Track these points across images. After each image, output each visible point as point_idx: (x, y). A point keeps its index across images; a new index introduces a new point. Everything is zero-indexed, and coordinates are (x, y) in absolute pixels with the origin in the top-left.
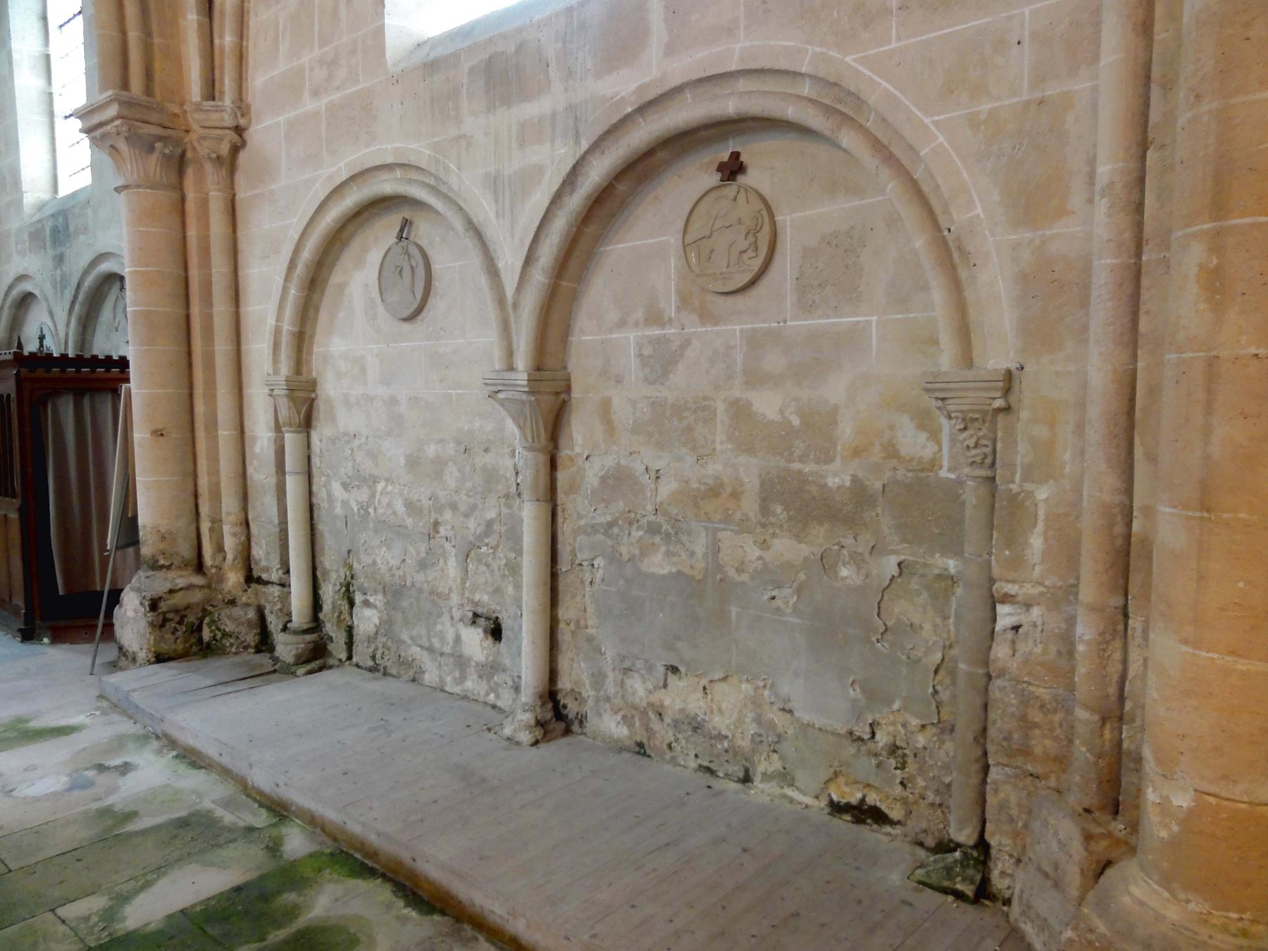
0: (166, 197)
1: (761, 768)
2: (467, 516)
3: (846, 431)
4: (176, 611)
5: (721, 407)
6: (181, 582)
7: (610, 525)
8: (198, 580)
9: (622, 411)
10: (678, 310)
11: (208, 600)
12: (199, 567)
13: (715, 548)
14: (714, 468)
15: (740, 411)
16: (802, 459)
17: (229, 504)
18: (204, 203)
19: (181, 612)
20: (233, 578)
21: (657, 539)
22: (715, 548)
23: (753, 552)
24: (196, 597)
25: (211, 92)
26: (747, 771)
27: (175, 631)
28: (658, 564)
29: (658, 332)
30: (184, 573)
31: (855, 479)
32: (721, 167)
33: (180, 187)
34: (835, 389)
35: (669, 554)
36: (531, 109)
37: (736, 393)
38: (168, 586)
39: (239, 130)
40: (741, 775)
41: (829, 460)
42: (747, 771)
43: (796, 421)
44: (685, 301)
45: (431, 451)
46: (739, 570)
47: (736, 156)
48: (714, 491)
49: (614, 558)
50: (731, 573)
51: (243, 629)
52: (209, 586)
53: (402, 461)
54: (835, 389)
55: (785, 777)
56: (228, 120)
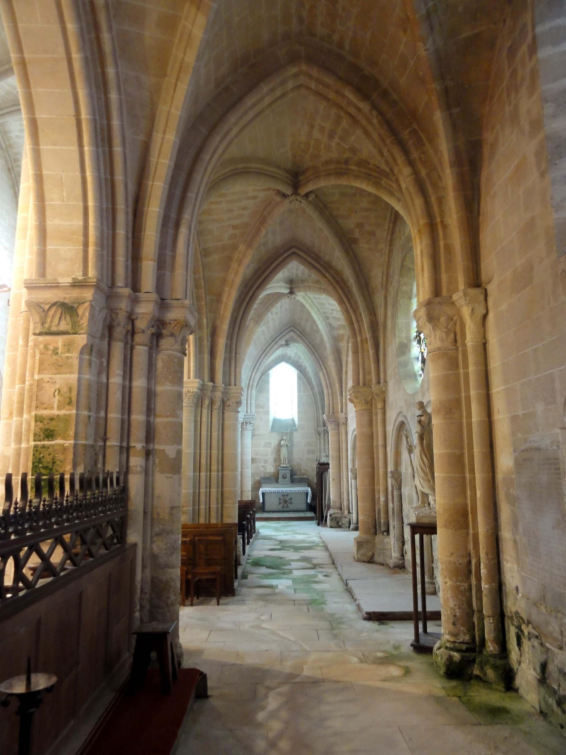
0: (336, 431)
4: (335, 517)
6: (336, 512)
8: (340, 512)
11: (342, 517)
12: (341, 509)
17: (345, 496)
18: (342, 433)
19: (336, 518)
20: (346, 512)
24: (339, 515)
25: (342, 412)
27: (334, 522)
30: (337, 510)
33: (339, 430)
38: (333, 512)
39: (347, 418)
51: (346, 523)
52: (341, 513)
56: (344, 417)
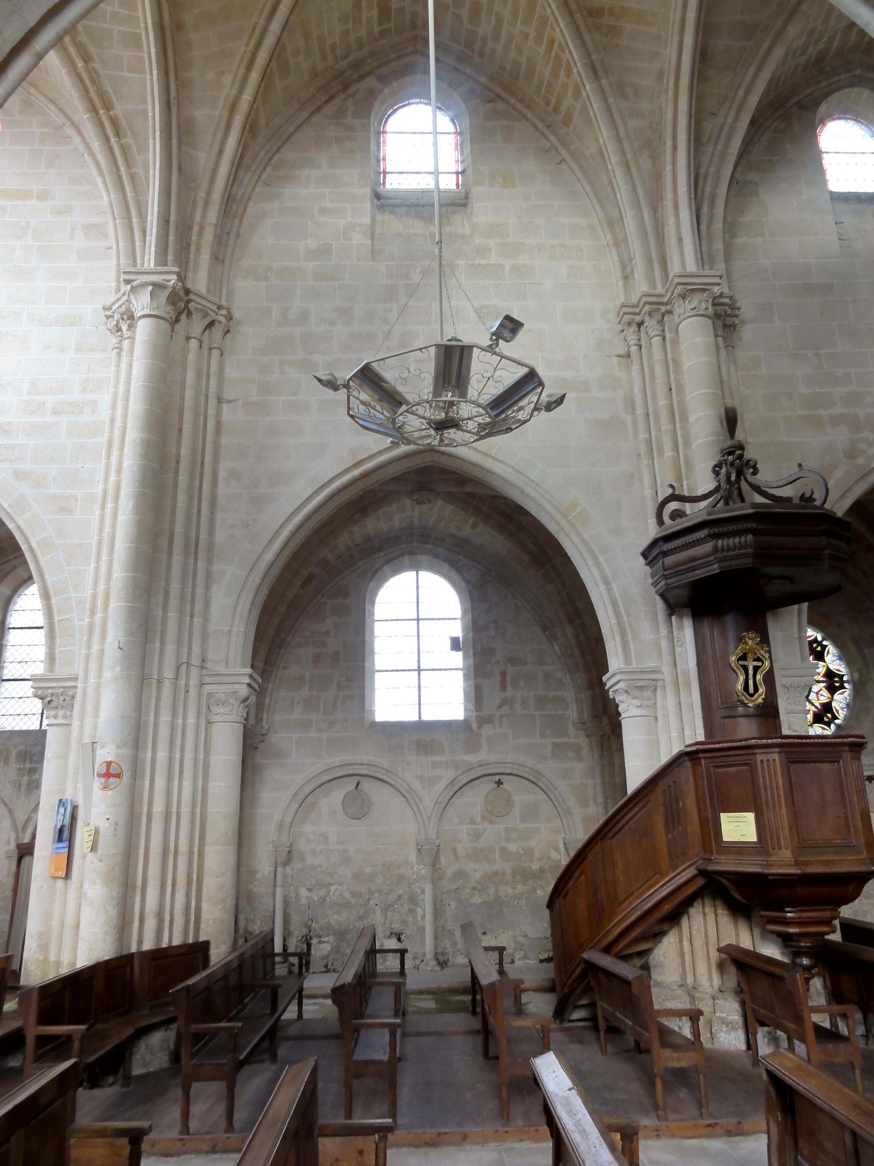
1: (517, 957)
2: (387, 894)
3: (537, 854)
5: (497, 849)
7: (457, 889)
9: (461, 851)
10: (482, 820)
13: (497, 891)
14: (496, 867)
15: (504, 850)
16: (525, 862)
21: (476, 891)
22: (497, 891)
23: (510, 891)
26: (512, 960)
28: (477, 900)
29: (474, 827)
31: (540, 866)
32: (496, 783)
34: (533, 843)
35: (480, 896)
36: (437, 758)
37: (503, 844)
40: (510, 961)
41: (533, 861)
42: (512, 960)
43: (522, 852)
44: (484, 818)
45: (368, 870)
46: (506, 897)
47: (499, 780)
48: (496, 874)
49: (459, 901)
50: (503, 898)
53: (350, 875)
54: (533, 843)
55: (525, 957)
